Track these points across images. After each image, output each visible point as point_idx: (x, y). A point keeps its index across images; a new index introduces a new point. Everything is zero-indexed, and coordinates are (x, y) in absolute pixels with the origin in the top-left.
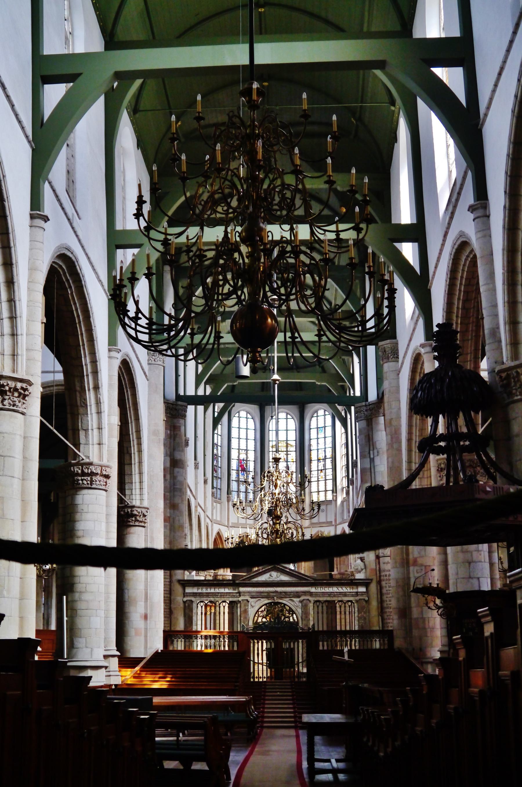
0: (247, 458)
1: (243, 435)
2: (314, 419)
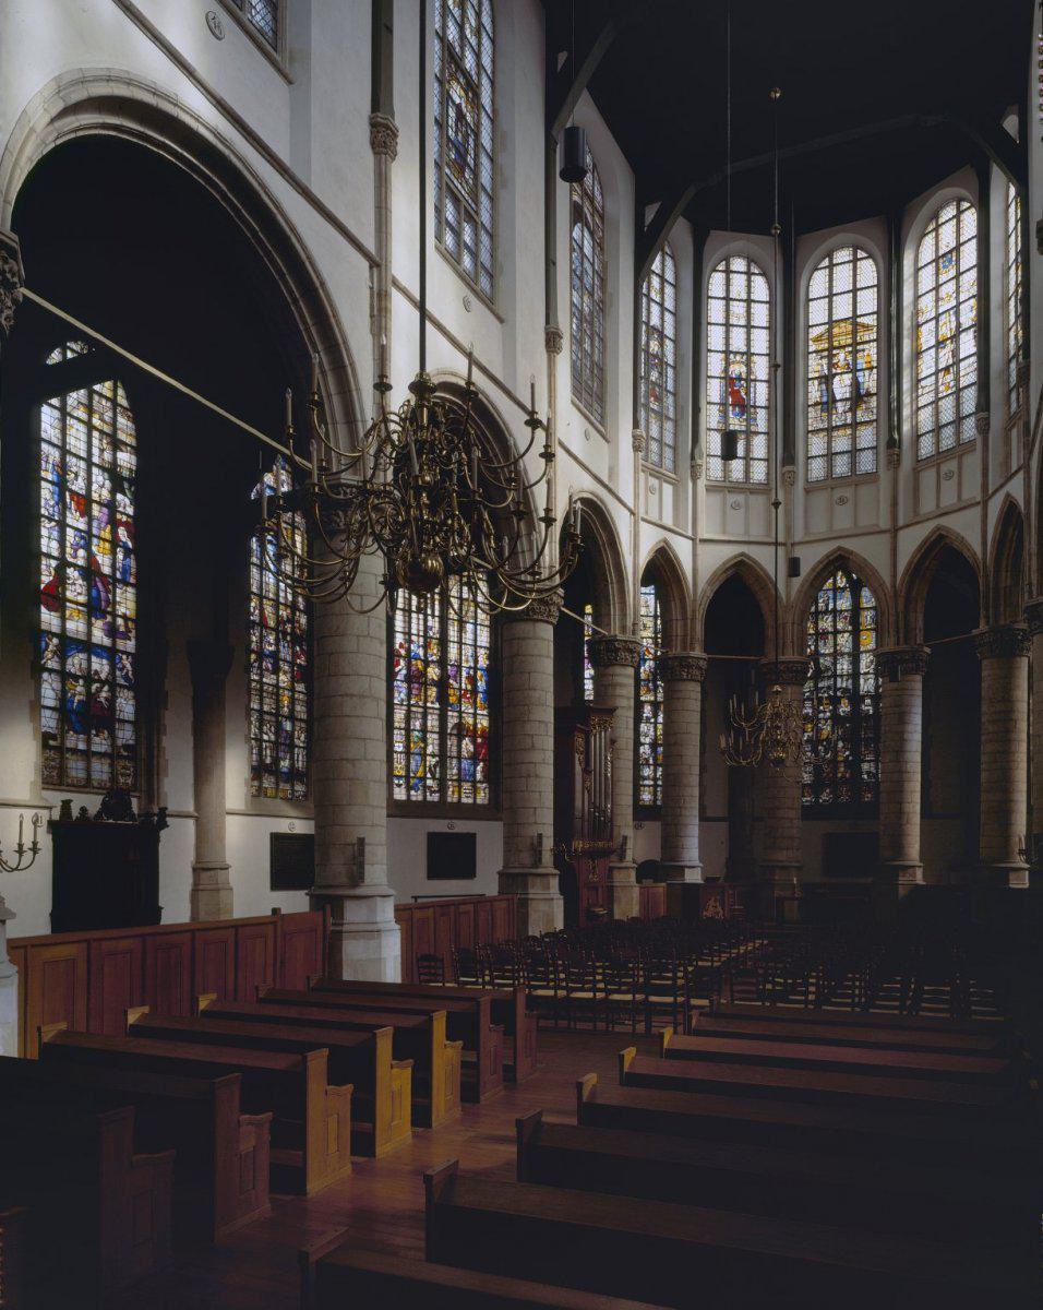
0: (749, 371)
1: (738, 309)
2: (929, 241)
